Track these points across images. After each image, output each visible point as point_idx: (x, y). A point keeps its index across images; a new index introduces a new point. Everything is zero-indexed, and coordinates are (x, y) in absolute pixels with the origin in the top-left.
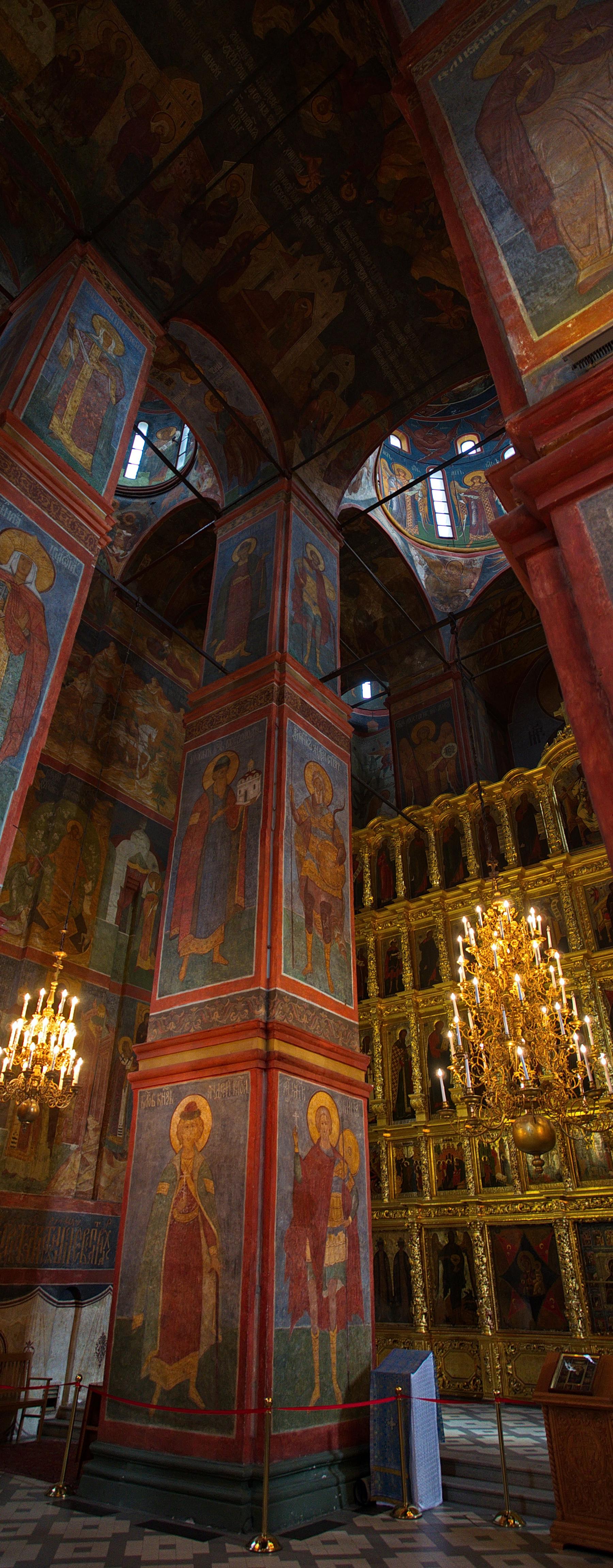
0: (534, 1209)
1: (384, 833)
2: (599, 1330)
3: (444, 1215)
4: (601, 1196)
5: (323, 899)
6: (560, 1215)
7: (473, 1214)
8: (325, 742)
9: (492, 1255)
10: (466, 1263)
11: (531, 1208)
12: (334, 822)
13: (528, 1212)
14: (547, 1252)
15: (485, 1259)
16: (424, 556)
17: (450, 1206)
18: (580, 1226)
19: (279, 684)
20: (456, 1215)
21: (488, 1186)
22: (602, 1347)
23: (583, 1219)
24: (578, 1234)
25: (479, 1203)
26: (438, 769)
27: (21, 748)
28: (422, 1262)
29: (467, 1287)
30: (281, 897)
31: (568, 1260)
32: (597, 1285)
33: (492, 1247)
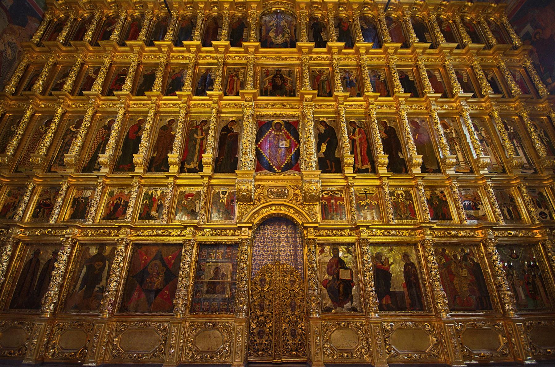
0: (172, 234)
2: (195, 311)
3: (99, 234)
4: (222, 228)
6: (190, 237)
7: (123, 234)
9: (130, 263)
10: (107, 268)
11: (170, 233)
13: (167, 235)
14: (173, 261)
15: (121, 265)
17: (106, 228)
18: (202, 245)
20: (109, 235)
21: (143, 219)
22: (194, 322)
23: (205, 242)
24: (199, 251)
25: (131, 228)
28: (67, 267)
29: (101, 284)
31: (186, 266)
32: (202, 282)
33: (132, 257)
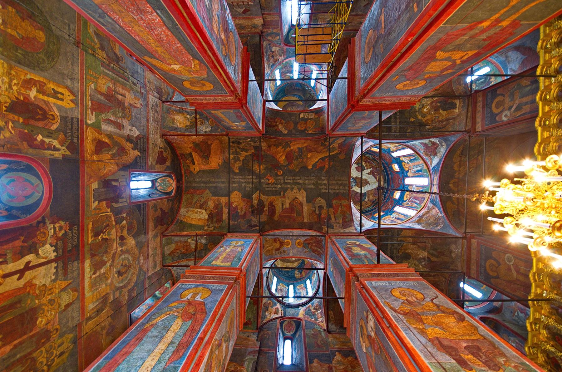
1: (542, 327)
5: (465, 345)
8: (397, 280)
12: (436, 305)
16: (412, 222)
19: (354, 276)
26: (518, 272)
27: (184, 354)
30: (419, 357)
